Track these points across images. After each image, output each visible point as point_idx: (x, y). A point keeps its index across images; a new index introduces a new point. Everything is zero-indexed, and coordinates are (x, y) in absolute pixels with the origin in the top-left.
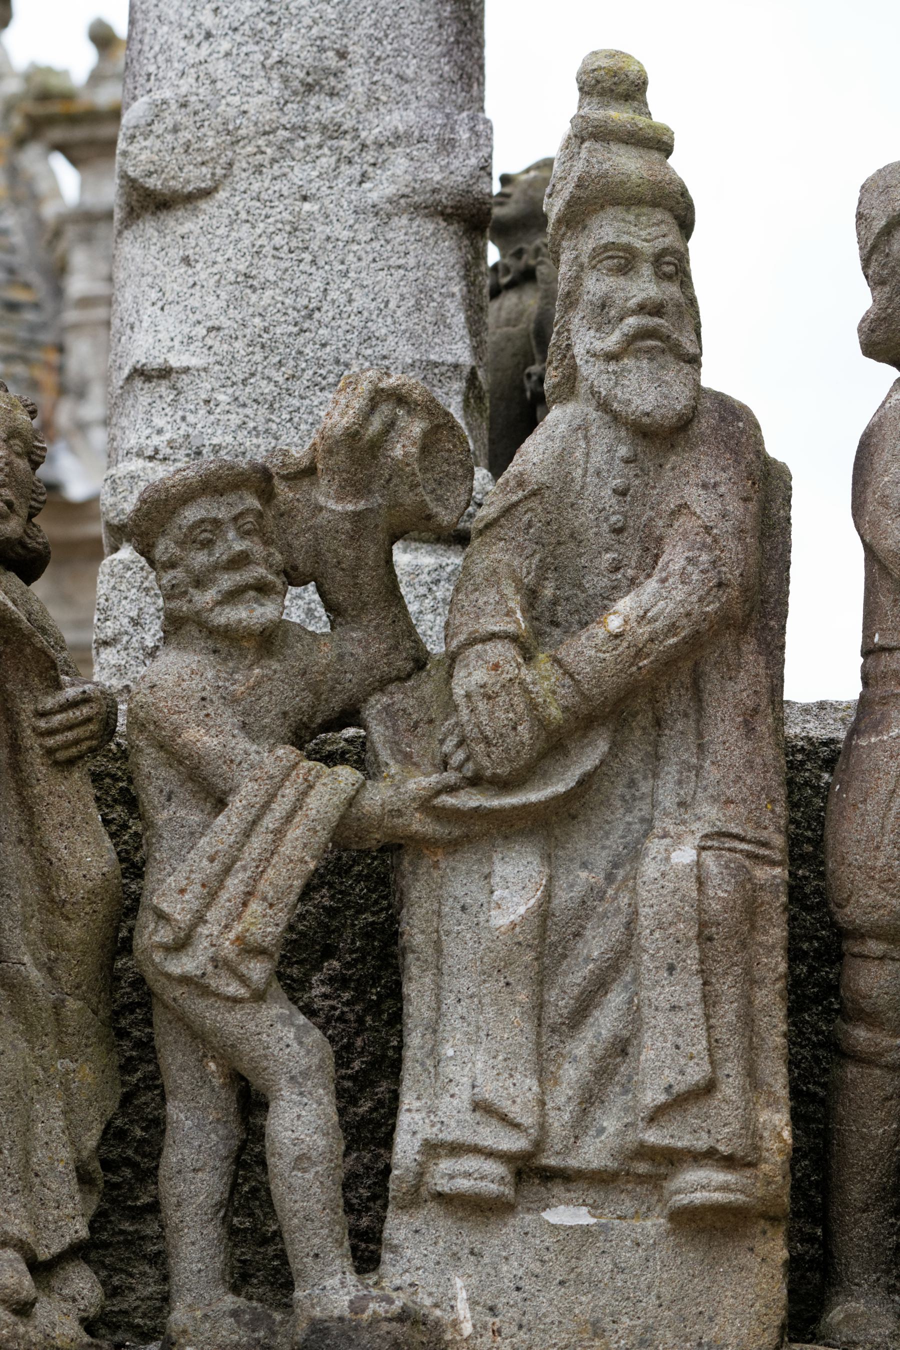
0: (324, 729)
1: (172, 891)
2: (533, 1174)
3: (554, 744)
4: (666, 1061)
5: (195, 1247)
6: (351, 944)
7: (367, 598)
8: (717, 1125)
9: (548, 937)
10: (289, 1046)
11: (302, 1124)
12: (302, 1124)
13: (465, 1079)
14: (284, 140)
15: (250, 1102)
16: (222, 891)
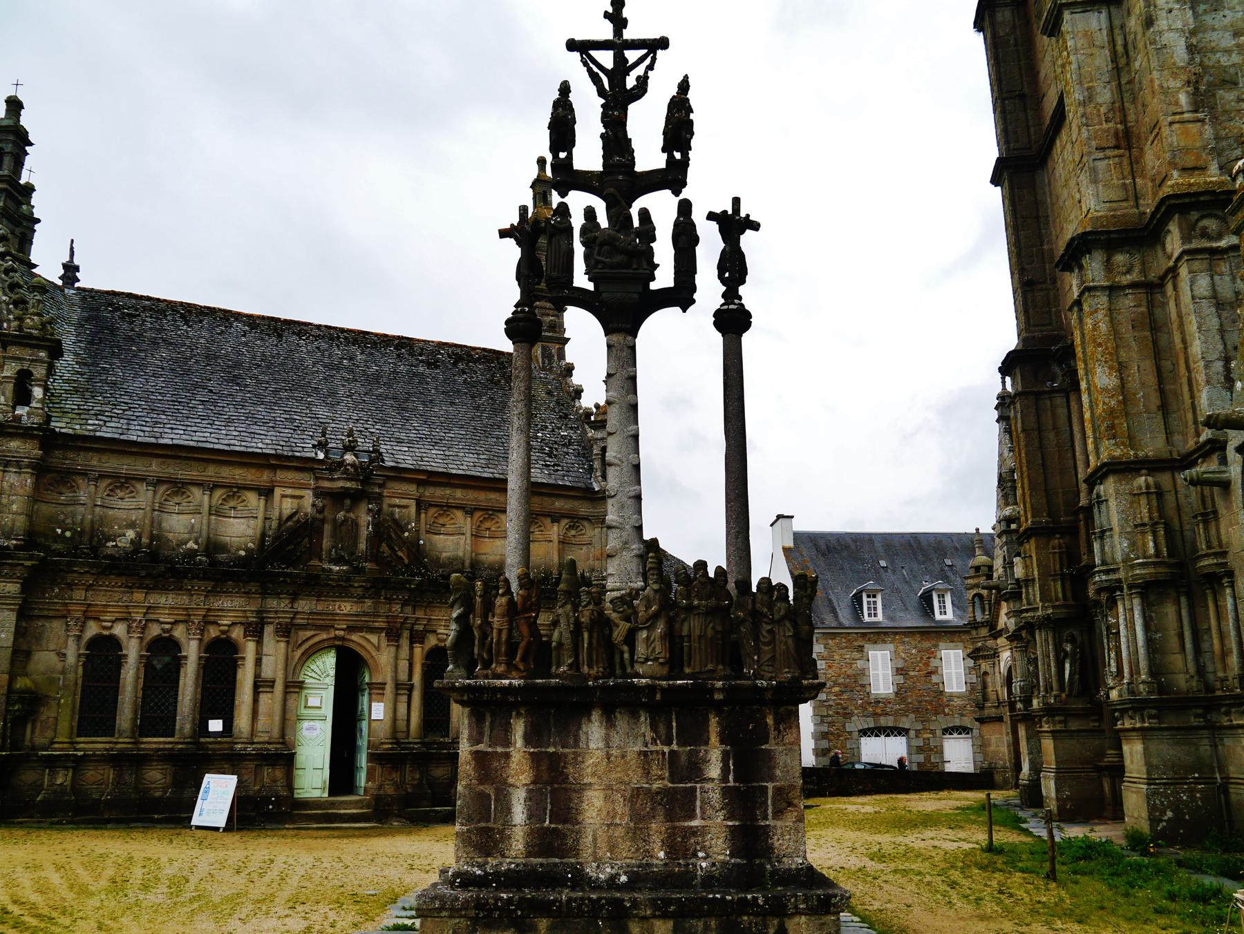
0: (627, 620)
1: (615, 635)
2: (647, 660)
3: (648, 620)
4: (658, 650)
5: (618, 667)
6: (630, 639)
7: (631, 605)
8: (662, 655)
9: (648, 638)
10: (625, 648)
11: (626, 656)
12: (626, 656)
13: (641, 649)
14: (623, 549)
15: (622, 653)
16: (619, 634)
